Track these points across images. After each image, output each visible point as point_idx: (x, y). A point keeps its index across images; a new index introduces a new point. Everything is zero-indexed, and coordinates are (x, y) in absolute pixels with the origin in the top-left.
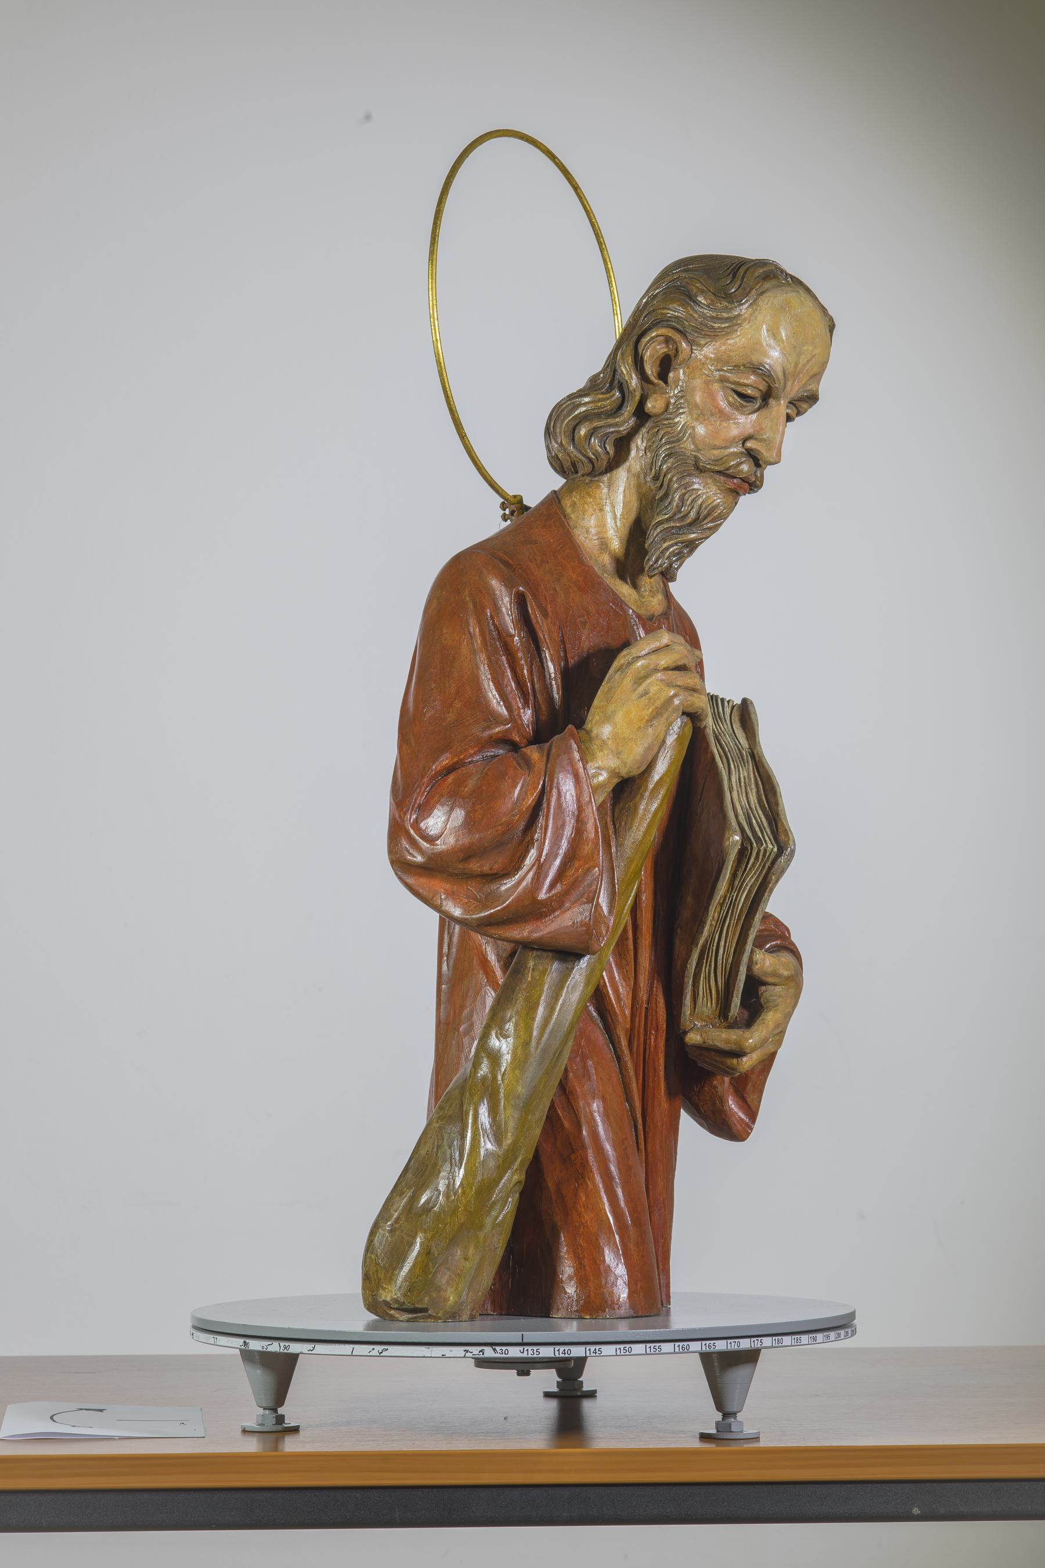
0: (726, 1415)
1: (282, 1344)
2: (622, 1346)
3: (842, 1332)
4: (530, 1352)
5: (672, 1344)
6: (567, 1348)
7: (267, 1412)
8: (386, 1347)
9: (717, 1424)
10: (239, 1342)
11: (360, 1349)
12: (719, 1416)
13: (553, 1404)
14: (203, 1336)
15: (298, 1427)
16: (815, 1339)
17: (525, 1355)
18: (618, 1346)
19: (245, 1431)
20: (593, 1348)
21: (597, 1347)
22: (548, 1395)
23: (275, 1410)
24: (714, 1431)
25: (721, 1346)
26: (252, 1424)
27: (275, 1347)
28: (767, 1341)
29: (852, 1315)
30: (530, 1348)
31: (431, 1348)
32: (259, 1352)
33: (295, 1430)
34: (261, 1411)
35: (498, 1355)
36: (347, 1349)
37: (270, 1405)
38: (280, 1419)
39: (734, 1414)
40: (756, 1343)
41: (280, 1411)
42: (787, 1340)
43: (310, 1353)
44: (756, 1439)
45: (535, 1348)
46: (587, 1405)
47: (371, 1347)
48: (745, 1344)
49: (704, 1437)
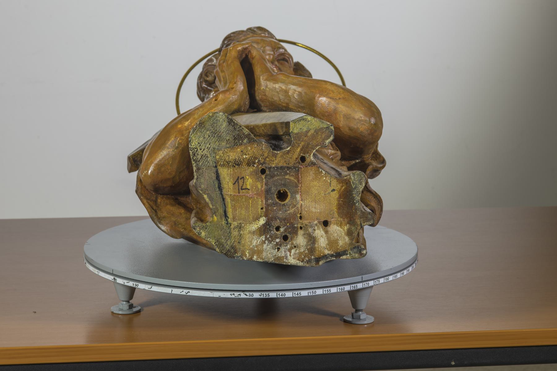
1: (135, 283)
2: (311, 291)
4: (265, 295)
7: (125, 303)
10: (111, 278)
12: (354, 310)
14: (91, 268)
15: (140, 310)
17: (262, 297)
19: (112, 312)
25: (360, 286)
27: (131, 284)
33: (139, 311)
37: (127, 300)
41: (130, 301)
48: (371, 283)
49: (345, 321)
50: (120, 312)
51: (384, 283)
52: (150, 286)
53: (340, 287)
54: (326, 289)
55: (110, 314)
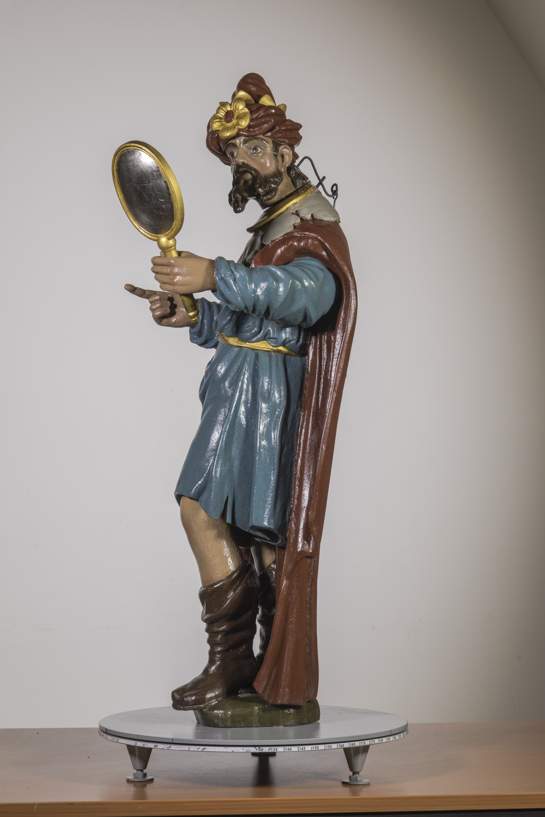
0: (354, 773)
2: (314, 746)
3: (405, 733)
5: (336, 745)
6: (290, 747)
7: (139, 772)
8: (206, 747)
9: (350, 778)
11: (192, 748)
12: (351, 773)
13: (256, 759)
14: (110, 737)
16: (395, 738)
17: (271, 751)
18: (312, 746)
19: (128, 781)
20: (301, 747)
21: (303, 747)
22: (254, 754)
23: (142, 771)
24: (348, 781)
25: (357, 744)
26: (131, 777)
28: (377, 741)
29: (407, 725)
30: (273, 748)
31: (227, 748)
32: (139, 747)
33: (152, 780)
34: (135, 771)
35: (258, 751)
36: (186, 748)
37: (141, 768)
38: (145, 775)
39: (358, 773)
40: (372, 742)
41: (145, 771)
42: (385, 740)
43: (168, 749)
44: (368, 785)
45: (275, 748)
46: (271, 760)
47: (198, 747)
48: (367, 743)
49: (344, 783)
50: (136, 780)
51: (379, 743)
52: (168, 746)
53: (340, 744)
54: (328, 745)
55: (126, 784)
